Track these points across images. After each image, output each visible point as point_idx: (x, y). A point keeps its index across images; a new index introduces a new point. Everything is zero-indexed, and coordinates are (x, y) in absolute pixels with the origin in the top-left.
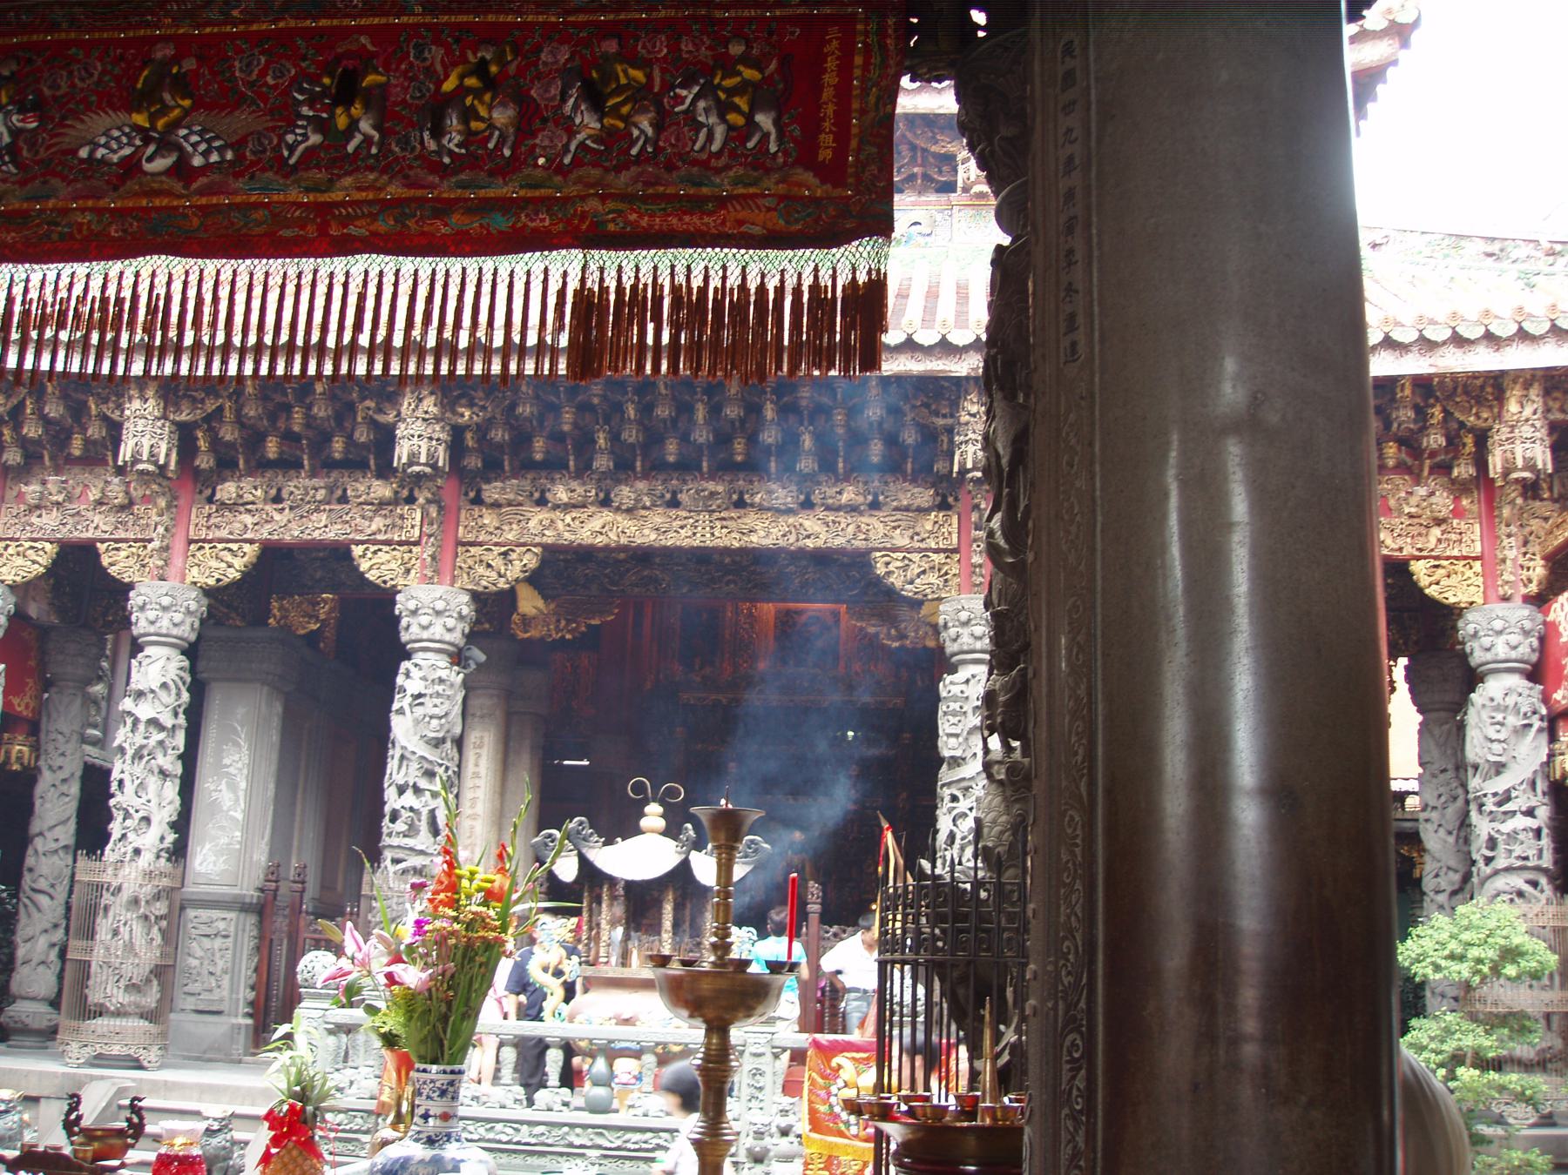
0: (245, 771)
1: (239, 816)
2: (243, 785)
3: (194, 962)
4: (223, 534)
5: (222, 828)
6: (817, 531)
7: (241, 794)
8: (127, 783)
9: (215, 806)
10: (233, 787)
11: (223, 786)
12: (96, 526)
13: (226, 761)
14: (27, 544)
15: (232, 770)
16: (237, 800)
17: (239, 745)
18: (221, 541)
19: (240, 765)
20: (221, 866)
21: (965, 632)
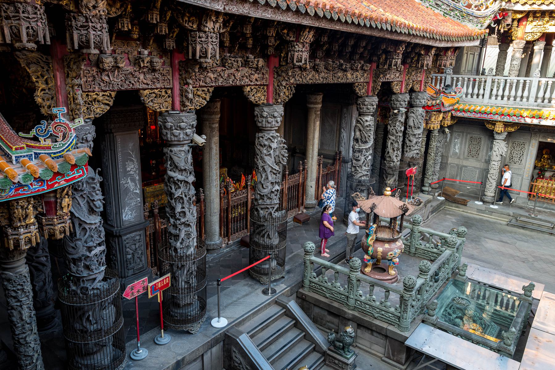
0: (137, 172)
1: (138, 191)
2: (137, 178)
3: (129, 257)
4: (201, 83)
5: (132, 199)
6: (350, 77)
7: (137, 182)
8: (187, 213)
9: (127, 190)
10: (133, 180)
11: (129, 181)
12: (141, 81)
13: (128, 169)
14: (101, 94)
15: (132, 173)
16: (136, 185)
17: (132, 161)
18: (200, 86)
19: (135, 169)
20: (134, 214)
21: (372, 107)
